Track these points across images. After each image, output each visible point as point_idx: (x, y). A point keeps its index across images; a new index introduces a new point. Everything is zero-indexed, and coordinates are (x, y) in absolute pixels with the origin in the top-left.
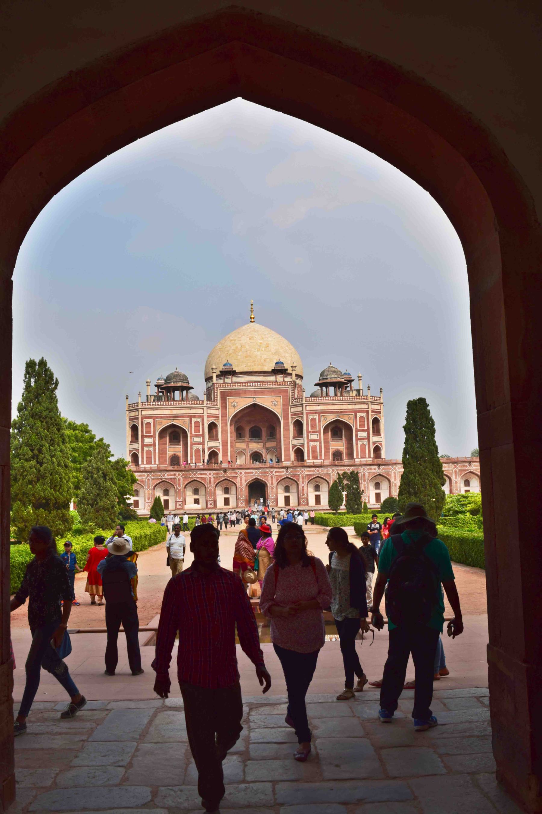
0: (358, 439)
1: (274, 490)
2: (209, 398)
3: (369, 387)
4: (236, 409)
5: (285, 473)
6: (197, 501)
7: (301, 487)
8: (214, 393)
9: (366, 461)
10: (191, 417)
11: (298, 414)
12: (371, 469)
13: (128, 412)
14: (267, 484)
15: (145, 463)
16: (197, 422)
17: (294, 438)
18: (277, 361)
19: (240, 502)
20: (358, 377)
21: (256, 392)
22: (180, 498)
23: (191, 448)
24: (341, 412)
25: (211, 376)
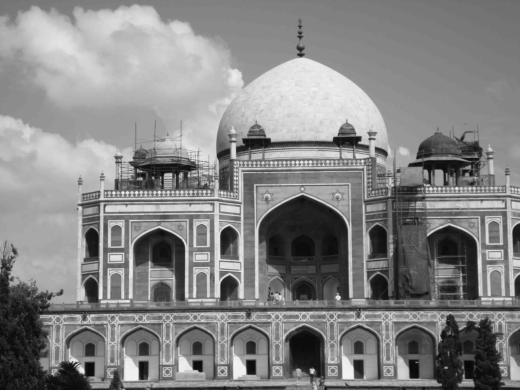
0: (486, 263)
1: (335, 349)
2: (223, 186)
4: (270, 206)
6: (198, 366)
7: (383, 345)
9: (504, 301)
10: (191, 218)
11: (379, 216)
12: (513, 317)
13: (80, 208)
15: (109, 296)
16: (202, 227)
19: (274, 369)
20: (488, 154)
22: (168, 359)
23: (191, 272)
24: (457, 214)
25: (227, 148)
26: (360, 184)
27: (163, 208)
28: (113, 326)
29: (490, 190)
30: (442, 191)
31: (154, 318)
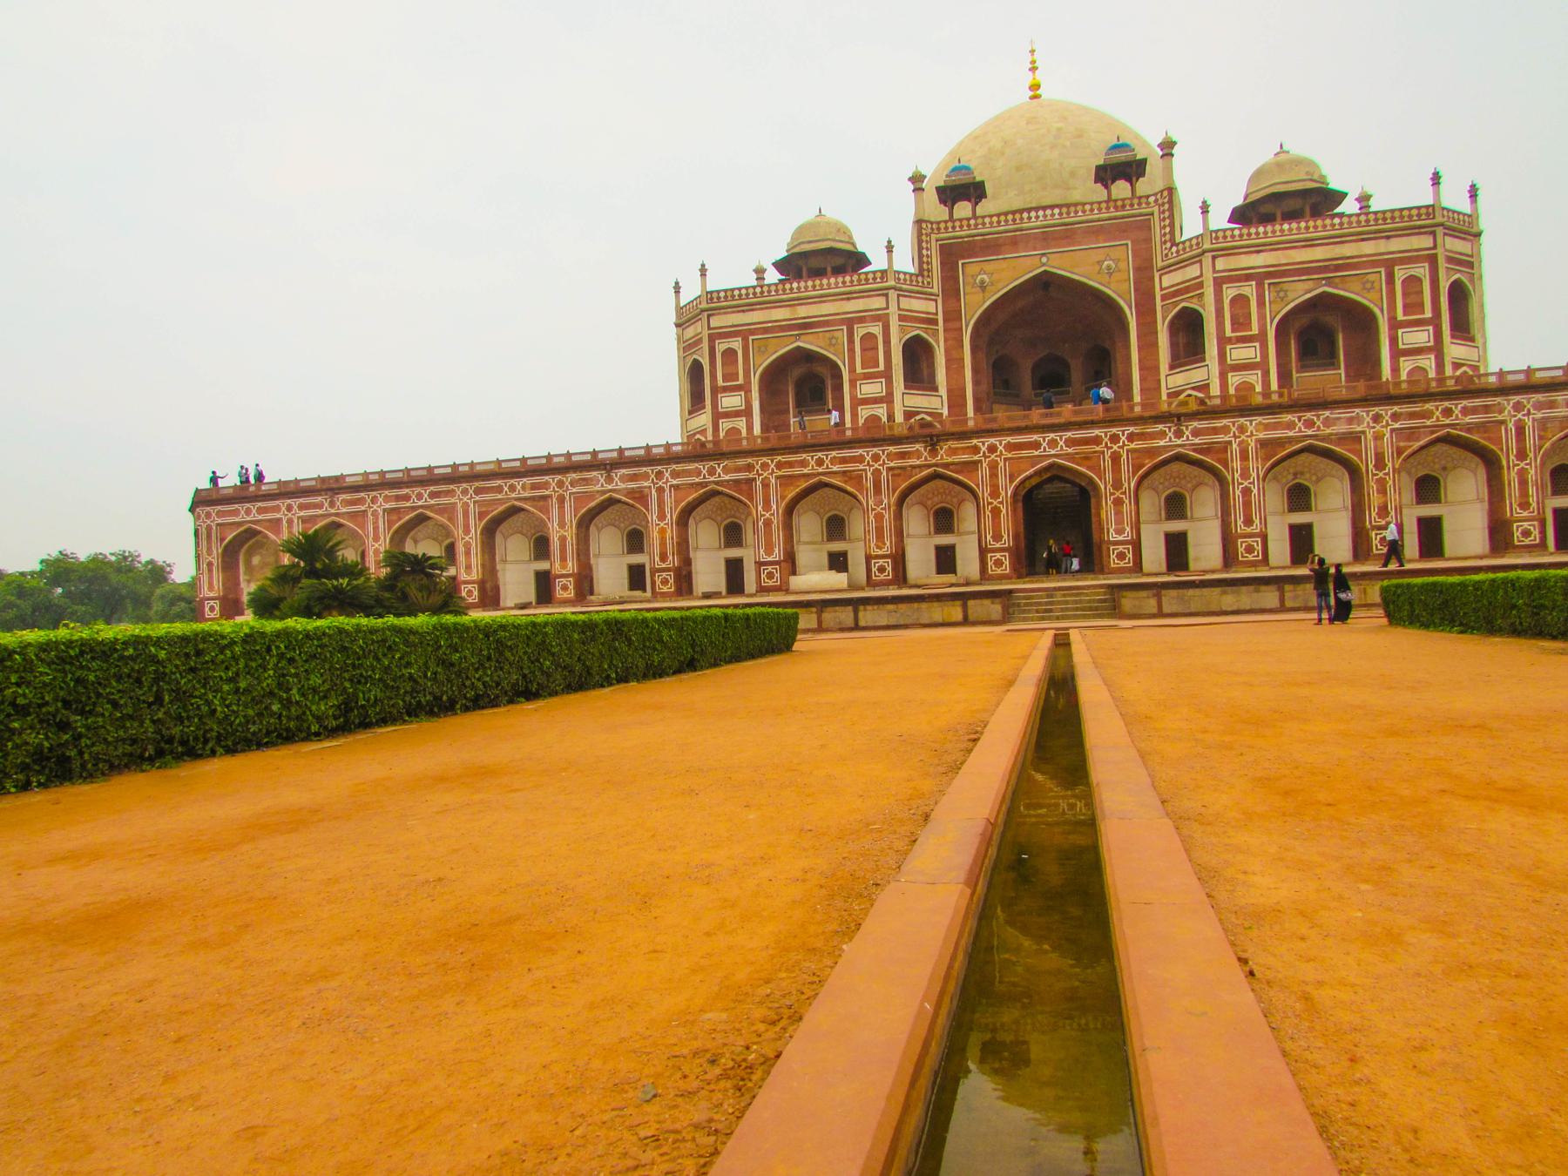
0: (1396, 353)
1: (1125, 508)
3: (1436, 179)
5: (1168, 440)
6: (838, 562)
8: (920, 249)
10: (850, 323)
11: (1187, 290)
12: (1552, 405)
14: (1096, 487)
16: (869, 337)
17: (1172, 367)
18: (1115, 142)
21: (1047, 238)
22: (769, 551)
23: (854, 415)
24: (1338, 268)
26: (1148, 240)
27: (802, 311)
28: (660, 490)
29: (1402, 217)
30: (1307, 228)
31: (738, 470)
